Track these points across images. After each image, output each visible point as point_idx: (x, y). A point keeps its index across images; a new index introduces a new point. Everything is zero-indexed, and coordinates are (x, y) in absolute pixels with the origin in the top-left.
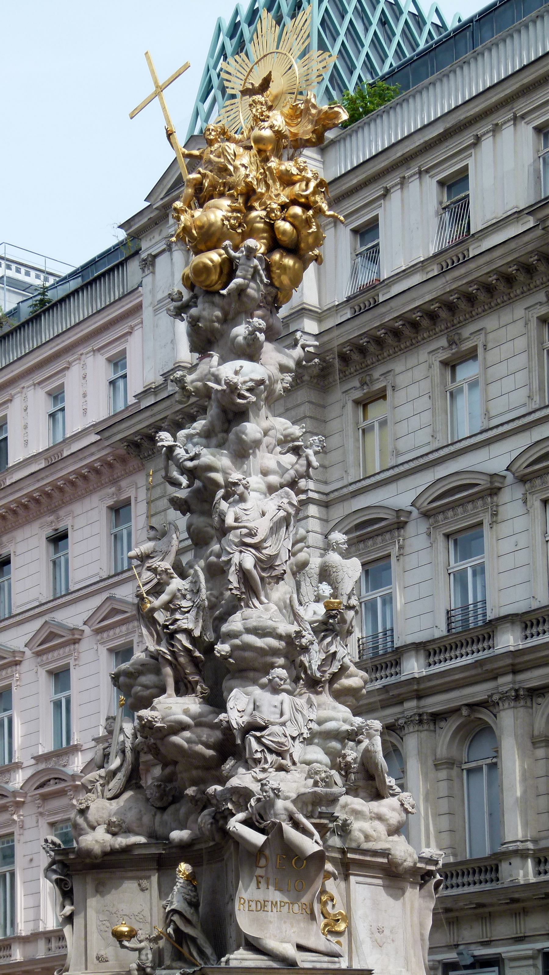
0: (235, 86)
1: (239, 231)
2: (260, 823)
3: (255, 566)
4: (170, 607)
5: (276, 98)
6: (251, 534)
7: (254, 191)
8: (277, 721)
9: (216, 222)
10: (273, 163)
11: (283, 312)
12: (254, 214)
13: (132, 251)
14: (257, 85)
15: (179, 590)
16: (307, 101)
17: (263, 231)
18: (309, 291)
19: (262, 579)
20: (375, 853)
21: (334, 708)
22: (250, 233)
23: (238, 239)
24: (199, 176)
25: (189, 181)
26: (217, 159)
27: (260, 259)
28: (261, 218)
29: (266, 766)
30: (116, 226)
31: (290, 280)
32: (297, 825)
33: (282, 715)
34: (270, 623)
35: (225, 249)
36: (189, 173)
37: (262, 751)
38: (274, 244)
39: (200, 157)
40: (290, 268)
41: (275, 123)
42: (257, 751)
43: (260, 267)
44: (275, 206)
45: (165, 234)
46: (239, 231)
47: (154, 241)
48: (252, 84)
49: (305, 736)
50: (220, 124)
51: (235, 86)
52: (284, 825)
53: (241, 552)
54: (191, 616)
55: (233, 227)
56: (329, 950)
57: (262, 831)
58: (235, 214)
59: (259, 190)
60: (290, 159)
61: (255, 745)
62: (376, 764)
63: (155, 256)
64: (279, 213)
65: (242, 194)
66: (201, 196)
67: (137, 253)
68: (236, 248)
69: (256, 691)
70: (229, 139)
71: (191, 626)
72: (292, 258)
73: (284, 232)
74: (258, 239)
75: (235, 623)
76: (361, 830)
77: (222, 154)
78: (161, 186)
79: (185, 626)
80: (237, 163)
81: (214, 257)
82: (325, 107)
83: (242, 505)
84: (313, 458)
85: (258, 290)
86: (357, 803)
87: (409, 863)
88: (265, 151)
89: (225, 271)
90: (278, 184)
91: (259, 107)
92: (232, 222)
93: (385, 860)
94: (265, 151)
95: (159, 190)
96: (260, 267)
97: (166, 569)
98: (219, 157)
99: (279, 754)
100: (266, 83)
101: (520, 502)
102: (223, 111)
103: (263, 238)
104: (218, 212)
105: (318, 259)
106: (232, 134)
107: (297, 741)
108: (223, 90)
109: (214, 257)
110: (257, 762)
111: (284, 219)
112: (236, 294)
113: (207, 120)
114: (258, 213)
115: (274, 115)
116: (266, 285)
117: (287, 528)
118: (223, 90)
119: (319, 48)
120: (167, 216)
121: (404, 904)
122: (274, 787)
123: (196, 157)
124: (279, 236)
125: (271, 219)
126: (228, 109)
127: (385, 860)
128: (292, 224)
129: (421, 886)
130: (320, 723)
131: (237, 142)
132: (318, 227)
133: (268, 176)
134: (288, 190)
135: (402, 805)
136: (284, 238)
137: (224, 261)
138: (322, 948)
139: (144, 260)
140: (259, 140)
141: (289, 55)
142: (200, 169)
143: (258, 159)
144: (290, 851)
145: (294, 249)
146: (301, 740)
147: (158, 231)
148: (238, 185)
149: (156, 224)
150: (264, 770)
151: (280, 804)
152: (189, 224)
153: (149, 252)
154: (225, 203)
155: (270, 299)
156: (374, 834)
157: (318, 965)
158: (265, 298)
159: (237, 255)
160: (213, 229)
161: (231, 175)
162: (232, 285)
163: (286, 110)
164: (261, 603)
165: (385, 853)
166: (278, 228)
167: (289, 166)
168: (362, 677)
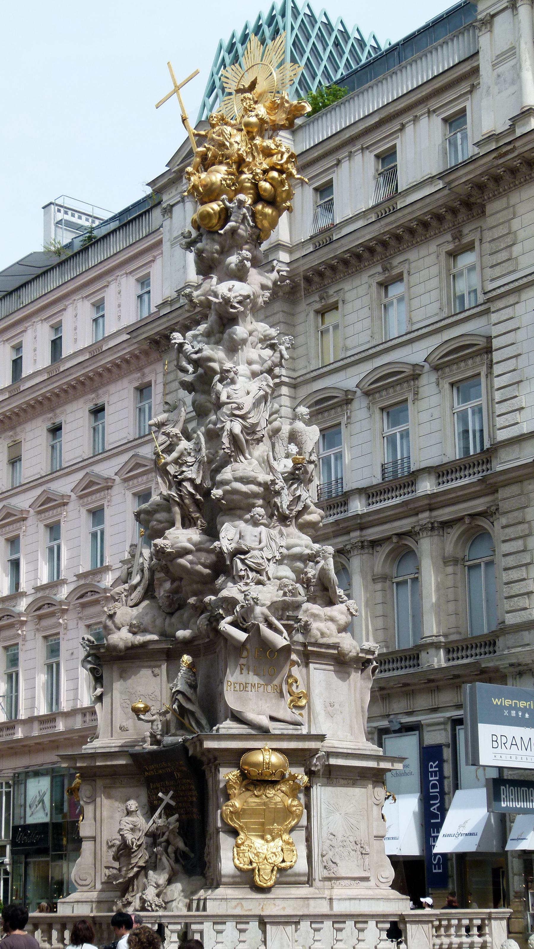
0: (232, 87)
1: (233, 188)
2: (243, 624)
3: (242, 432)
4: (179, 462)
5: (261, 95)
6: (239, 408)
7: (244, 160)
8: (257, 547)
9: (217, 182)
10: (258, 141)
11: (264, 246)
12: (243, 177)
13: (156, 202)
14: (247, 86)
15: (185, 449)
16: (282, 98)
17: (250, 188)
18: (283, 232)
19: (247, 441)
20: (328, 646)
21: (299, 537)
22: (241, 190)
23: (232, 194)
24: (204, 149)
25: (197, 152)
26: (218, 138)
27: (247, 209)
28: (249, 179)
29: (248, 581)
30: (145, 184)
31: (269, 223)
32: (270, 626)
33: (260, 542)
34: (252, 474)
35: (223, 201)
36: (198, 147)
38: (258, 198)
39: (205, 136)
40: (269, 215)
41: (259, 113)
42: (241, 570)
43: (247, 214)
44: (259, 171)
45: (179, 190)
46: (233, 188)
47: (171, 195)
48: (243, 86)
49: (277, 558)
50: (220, 113)
51: (232, 87)
52: (261, 625)
53: (231, 421)
54: (194, 468)
55: (229, 186)
56: (293, 720)
57: (245, 630)
58: (230, 177)
59: (248, 160)
60: (270, 138)
61: (240, 565)
62: (329, 579)
63: (172, 206)
64: (261, 176)
65: (235, 162)
66: (206, 163)
67: (159, 203)
68: (231, 201)
69: (241, 524)
70: (226, 124)
71: (194, 476)
72: (271, 208)
73: (265, 190)
74: (246, 194)
75: (227, 474)
77: (221, 134)
78: (178, 157)
79: (190, 476)
80: (232, 140)
81: (215, 207)
82: (295, 102)
83: (233, 387)
84: (284, 352)
85: (246, 231)
86: (315, 608)
87: (353, 654)
88: (252, 132)
89: (223, 217)
90: (261, 156)
91: (248, 101)
92: (228, 182)
93: (335, 652)
94: (252, 132)
95: (176, 159)
96: (247, 214)
97: (176, 434)
98: (219, 136)
99: (258, 572)
100: (253, 85)
101: (434, 385)
102: (223, 104)
103: (250, 194)
104: (219, 175)
105: (289, 209)
106: (229, 120)
107: (271, 562)
108: (223, 89)
109: (215, 207)
110: (242, 578)
111: (265, 180)
112: (230, 234)
113: (211, 110)
114: (247, 176)
115: (259, 107)
116: (252, 227)
117: (265, 403)
118: (223, 89)
119: (291, 61)
120: (182, 177)
121: (349, 684)
122: (254, 597)
123: (203, 136)
124: (262, 193)
125: (255, 180)
126: (226, 102)
127: (335, 652)
128: (271, 184)
129: (362, 671)
130: (288, 549)
131: (232, 126)
132: (289, 185)
133: (254, 150)
134: (268, 160)
135: (349, 609)
136: (265, 194)
137: (222, 209)
138: (288, 718)
139: (165, 209)
140: (247, 125)
141: (270, 66)
142: (206, 144)
143: (247, 138)
144: (265, 645)
145: (272, 202)
146: (275, 561)
147: (175, 188)
148: (232, 156)
149: (174, 183)
150: (247, 584)
151: (258, 610)
152: (197, 183)
153: (168, 203)
154: (223, 168)
155: (254, 237)
156: (328, 632)
157: (285, 732)
158: (251, 236)
159: (231, 205)
160: (214, 187)
161: (227, 149)
162: (227, 227)
163: (268, 104)
164: (246, 459)
165: (335, 646)
166: (261, 187)
167: (269, 143)
168: (319, 514)
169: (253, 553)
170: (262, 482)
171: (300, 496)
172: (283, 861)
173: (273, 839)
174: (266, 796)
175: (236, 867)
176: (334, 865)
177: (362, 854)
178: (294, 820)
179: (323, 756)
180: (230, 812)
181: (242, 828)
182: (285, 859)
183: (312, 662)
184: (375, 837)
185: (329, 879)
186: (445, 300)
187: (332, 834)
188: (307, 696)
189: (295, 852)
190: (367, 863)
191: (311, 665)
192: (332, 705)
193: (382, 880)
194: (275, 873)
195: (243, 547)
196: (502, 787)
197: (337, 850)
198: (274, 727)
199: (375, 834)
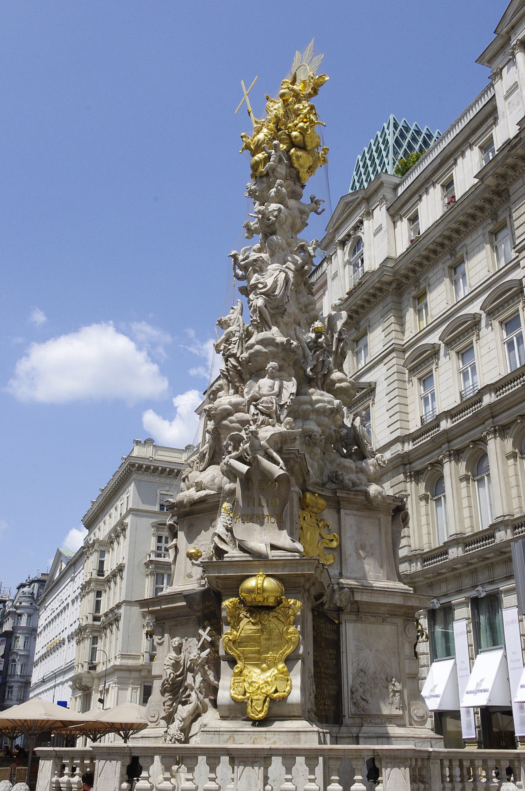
2: (247, 458)
3: (265, 306)
37: (257, 414)
49: (288, 404)
71: (235, 352)
76: (349, 480)
99: (269, 416)
144: (266, 475)
169: (264, 398)
172: (276, 691)
173: (269, 668)
175: (233, 699)
176: (363, 703)
184: (407, 674)
186: (491, 264)
187: (362, 670)
189: (289, 682)
191: (341, 510)
194: (267, 704)
197: (367, 687)
198: (273, 554)
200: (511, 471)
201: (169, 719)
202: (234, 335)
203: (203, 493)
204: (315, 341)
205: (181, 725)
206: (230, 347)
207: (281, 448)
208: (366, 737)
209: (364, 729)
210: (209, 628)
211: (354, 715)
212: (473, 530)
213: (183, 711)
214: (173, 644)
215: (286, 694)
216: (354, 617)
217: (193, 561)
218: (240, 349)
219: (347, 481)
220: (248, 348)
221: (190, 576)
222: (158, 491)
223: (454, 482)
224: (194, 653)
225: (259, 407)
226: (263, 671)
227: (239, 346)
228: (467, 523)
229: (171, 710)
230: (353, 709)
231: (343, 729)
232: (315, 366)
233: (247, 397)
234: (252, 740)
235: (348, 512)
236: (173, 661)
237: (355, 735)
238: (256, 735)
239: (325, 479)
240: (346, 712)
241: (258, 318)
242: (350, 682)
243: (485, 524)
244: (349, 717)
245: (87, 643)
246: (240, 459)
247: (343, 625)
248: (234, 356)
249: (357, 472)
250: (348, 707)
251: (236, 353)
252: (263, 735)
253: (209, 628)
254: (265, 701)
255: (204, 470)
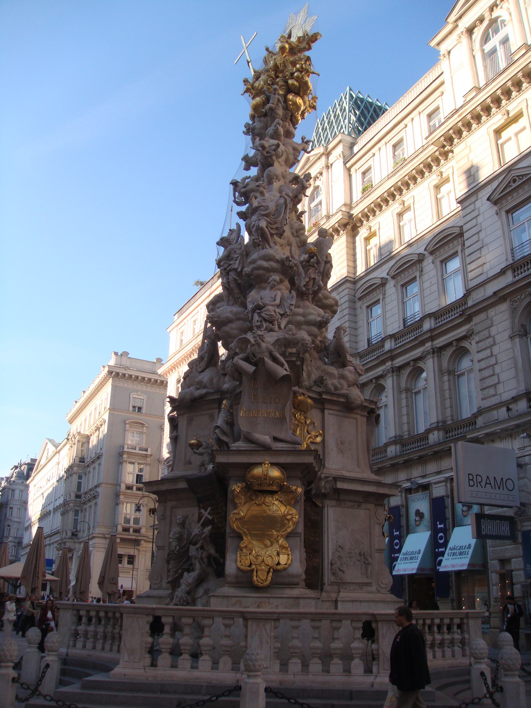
20: (339, 395)
32: (275, 359)
37: (261, 321)
57: (255, 364)
71: (236, 266)
76: (332, 384)
87: (358, 402)
99: (271, 322)
130: (304, 317)
135: (356, 369)
138: (289, 439)
144: (271, 376)
156: (339, 386)
165: (346, 396)
169: (267, 307)
170: (279, 259)
171: (314, 279)
173: (272, 545)
174: (265, 504)
175: (238, 568)
176: (341, 573)
177: (364, 563)
178: (290, 527)
179: (331, 480)
180: (236, 519)
181: (245, 532)
182: (281, 562)
183: (326, 409)
184: (376, 550)
185: (338, 584)
187: (340, 546)
188: (323, 435)
190: (369, 571)
192: (342, 443)
193: (382, 586)
194: (271, 574)
195: (260, 303)
196: (482, 520)
199: (377, 547)
200: (446, 386)
201: (175, 584)
202: (235, 252)
203: (204, 391)
204: (308, 261)
205: (187, 589)
206: (231, 262)
207: (285, 352)
208: (343, 601)
209: (341, 594)
210: (209, 509)
211: (333, 583)
212: (409, 434)
213: (189, 578)
214: (178, 520)
215: (287, 566)
216: (334, 503)
217: (195, 450)
218: (241, 265)
219: (330, 386)
220: (251, 263)
221: (190, 463)
222: (131, 394)
223: (396, 394)
224: (196, 530)
225: (263, 315)
226: (266, 546)
227: (240, 262)
228: (405, 427)
229: (176, 575)
230: (332, 578)
231: (324, 594)
232: (307, 282)
233: (250, 306)
234: (257, 604)
235: (331, 412)
236: (177, 535)
237: (334, 599)
238: (260, 600)
239: (312, 383)
240: (326, 581)
241: (260, 237)
242: (330, 556)
243: (422, 429)
244: (328, 584)
245: (71, 515)
246: (246, 359)
247: (326, 509)
248: (235, 270)
249: (339, 378)
250: (328, 577)
251: (237, 268)
252: (267, 600)
253: (209, 509)
254: (268, 572)
255: (203, 371)
